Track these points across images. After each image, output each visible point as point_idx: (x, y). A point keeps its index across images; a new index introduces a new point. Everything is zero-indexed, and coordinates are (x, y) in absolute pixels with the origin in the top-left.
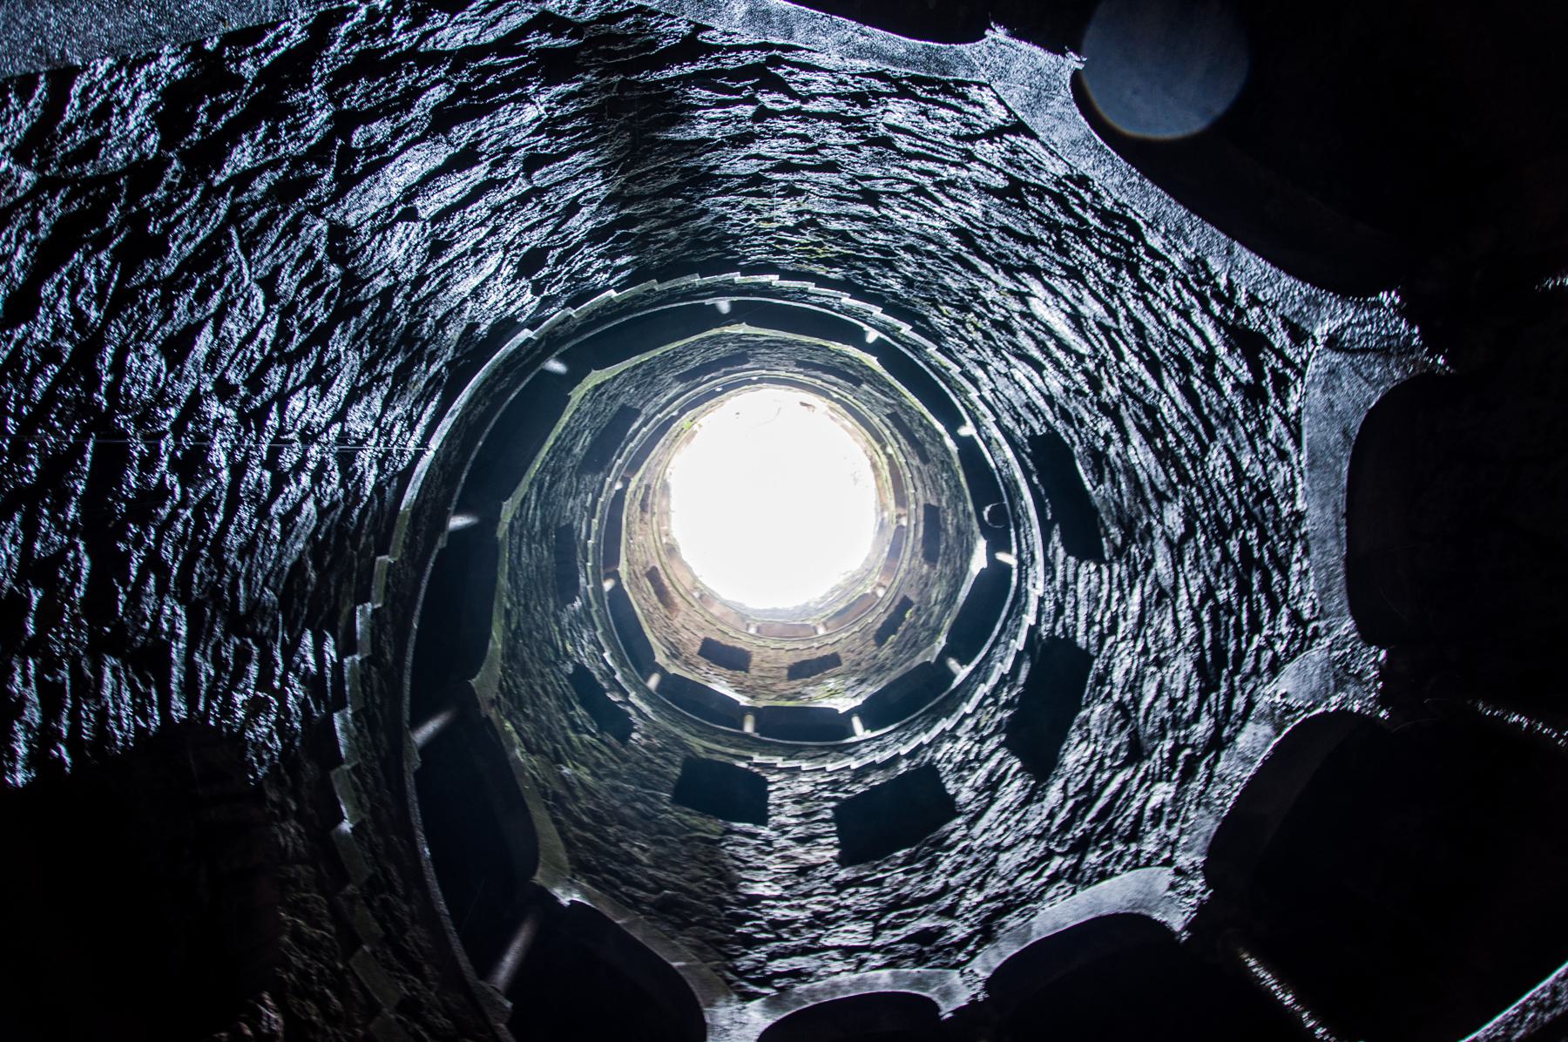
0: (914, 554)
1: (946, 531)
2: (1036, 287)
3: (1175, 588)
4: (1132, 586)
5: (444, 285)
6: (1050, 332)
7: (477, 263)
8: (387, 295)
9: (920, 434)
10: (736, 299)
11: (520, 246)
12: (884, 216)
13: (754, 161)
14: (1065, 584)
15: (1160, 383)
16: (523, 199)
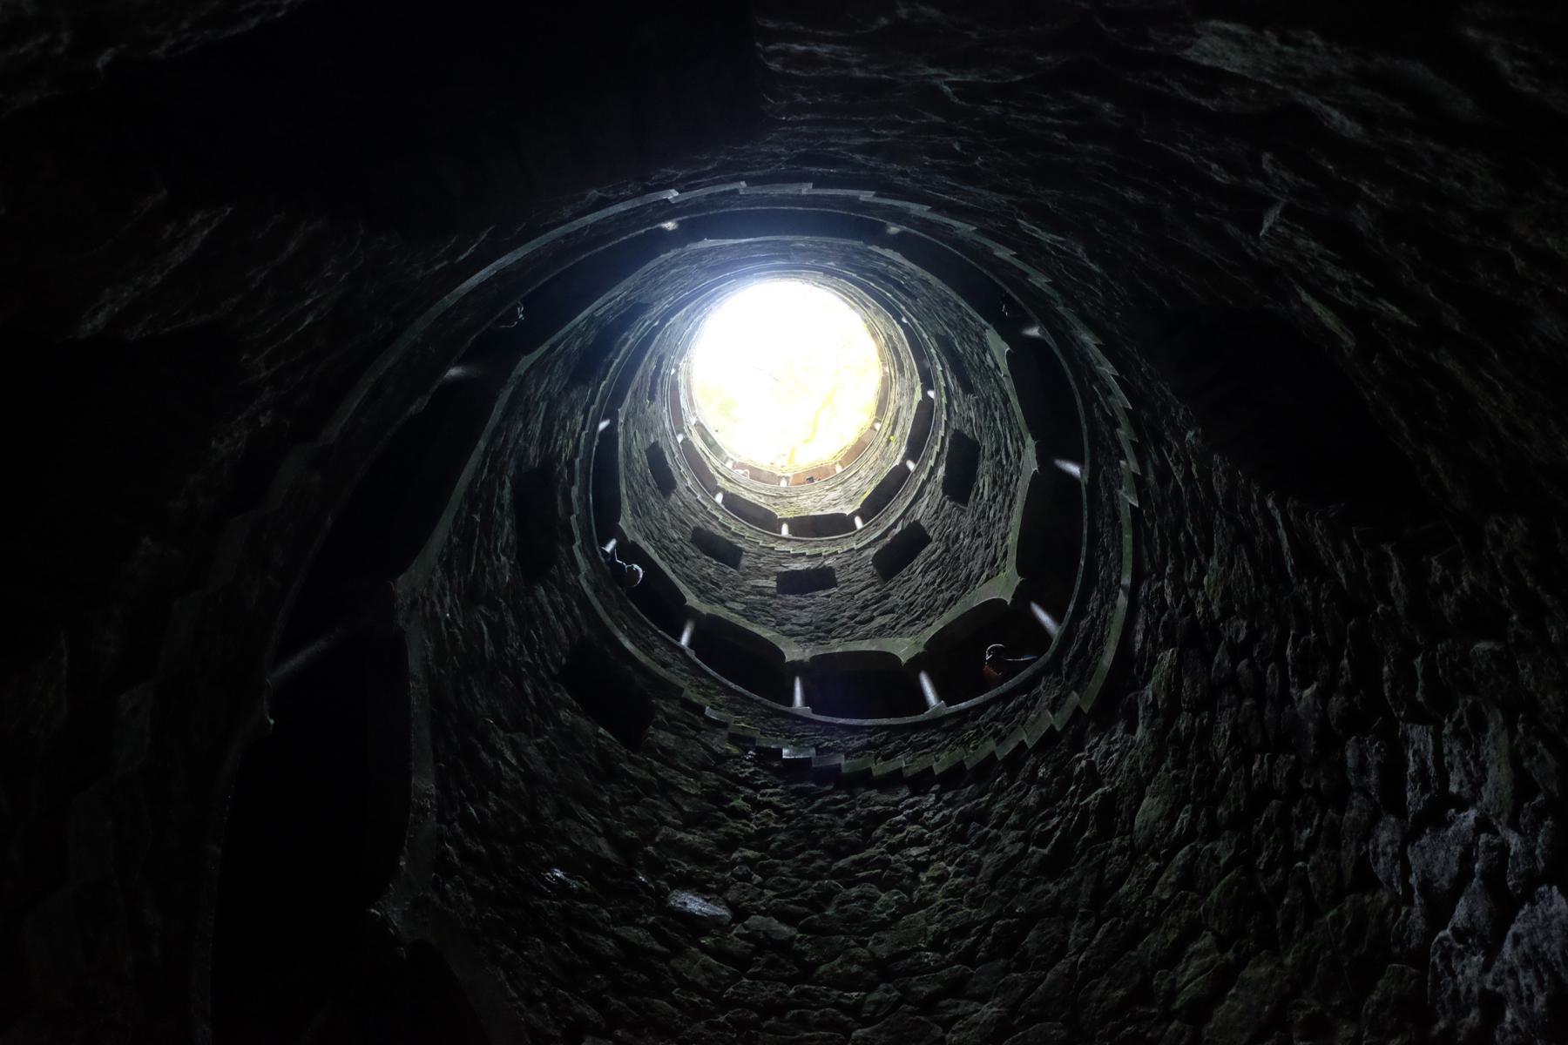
0: (664, 434)
1: (653, 494)
2: (736, 945)
3: (516, 748)
4: (536, 693)
5: (1171, 817)
6: (701, 889)
7: (1150, 839)
8: (1214, 833)
9: (711, 568)
10: (920, 717)
11: (1121, 851)
12: (863, 944)
13: (977, 990)
14: (570, 611)
15: (620, 941)
16: (1136, 934)
